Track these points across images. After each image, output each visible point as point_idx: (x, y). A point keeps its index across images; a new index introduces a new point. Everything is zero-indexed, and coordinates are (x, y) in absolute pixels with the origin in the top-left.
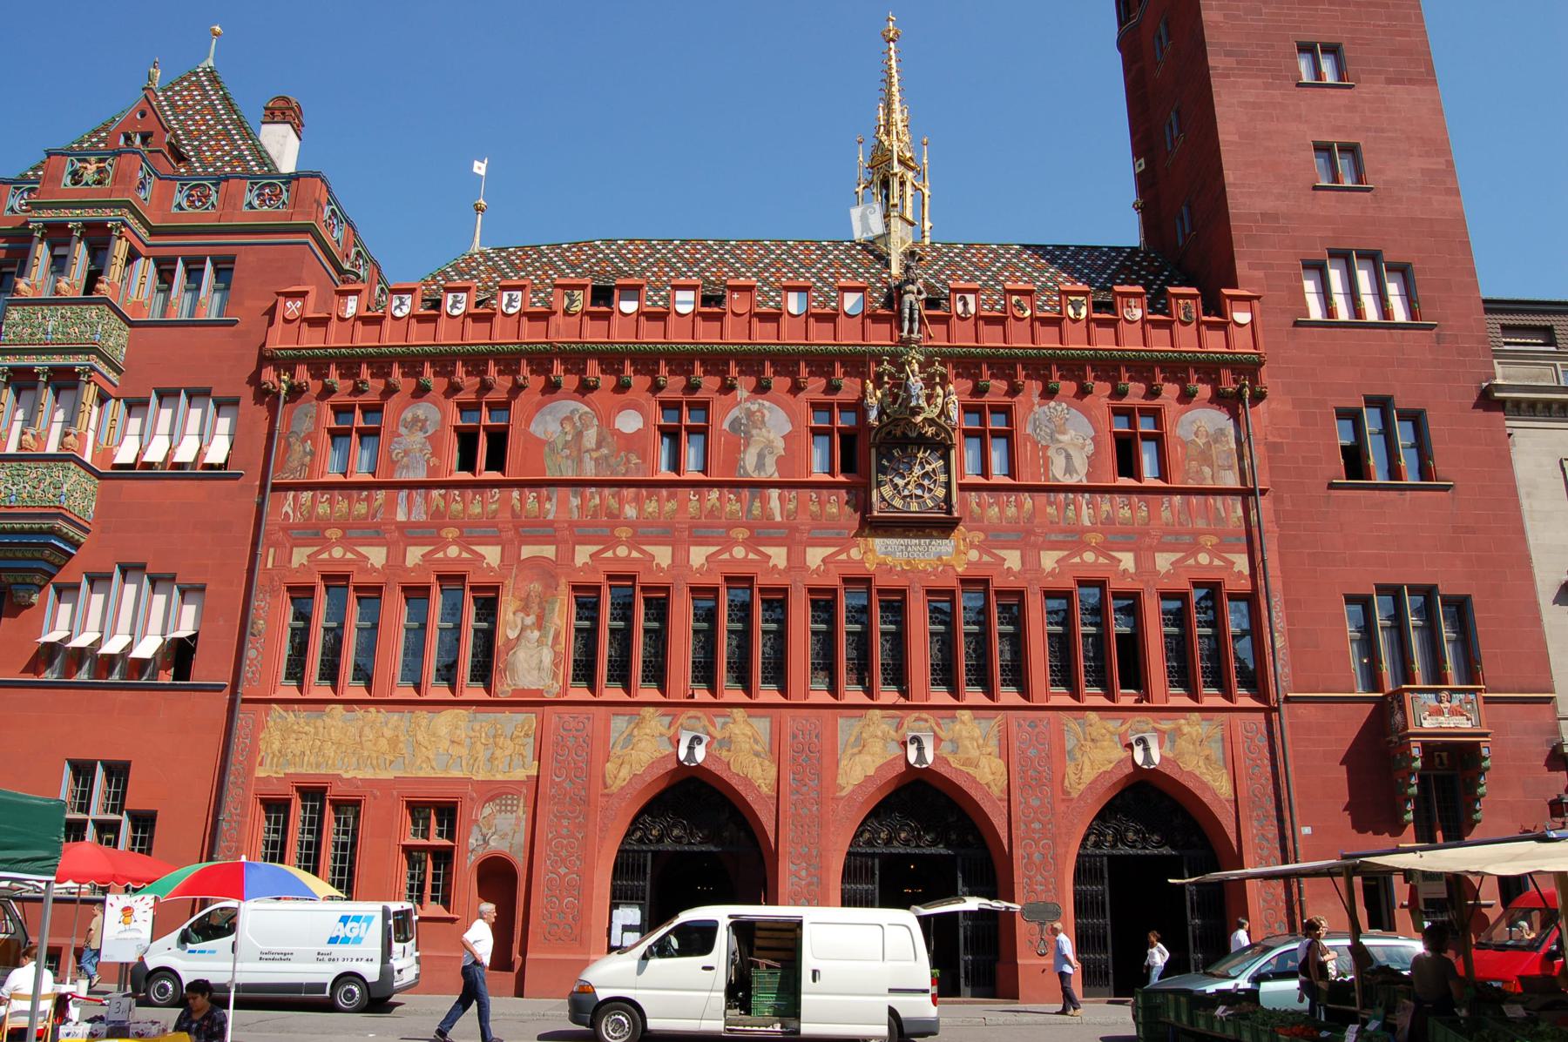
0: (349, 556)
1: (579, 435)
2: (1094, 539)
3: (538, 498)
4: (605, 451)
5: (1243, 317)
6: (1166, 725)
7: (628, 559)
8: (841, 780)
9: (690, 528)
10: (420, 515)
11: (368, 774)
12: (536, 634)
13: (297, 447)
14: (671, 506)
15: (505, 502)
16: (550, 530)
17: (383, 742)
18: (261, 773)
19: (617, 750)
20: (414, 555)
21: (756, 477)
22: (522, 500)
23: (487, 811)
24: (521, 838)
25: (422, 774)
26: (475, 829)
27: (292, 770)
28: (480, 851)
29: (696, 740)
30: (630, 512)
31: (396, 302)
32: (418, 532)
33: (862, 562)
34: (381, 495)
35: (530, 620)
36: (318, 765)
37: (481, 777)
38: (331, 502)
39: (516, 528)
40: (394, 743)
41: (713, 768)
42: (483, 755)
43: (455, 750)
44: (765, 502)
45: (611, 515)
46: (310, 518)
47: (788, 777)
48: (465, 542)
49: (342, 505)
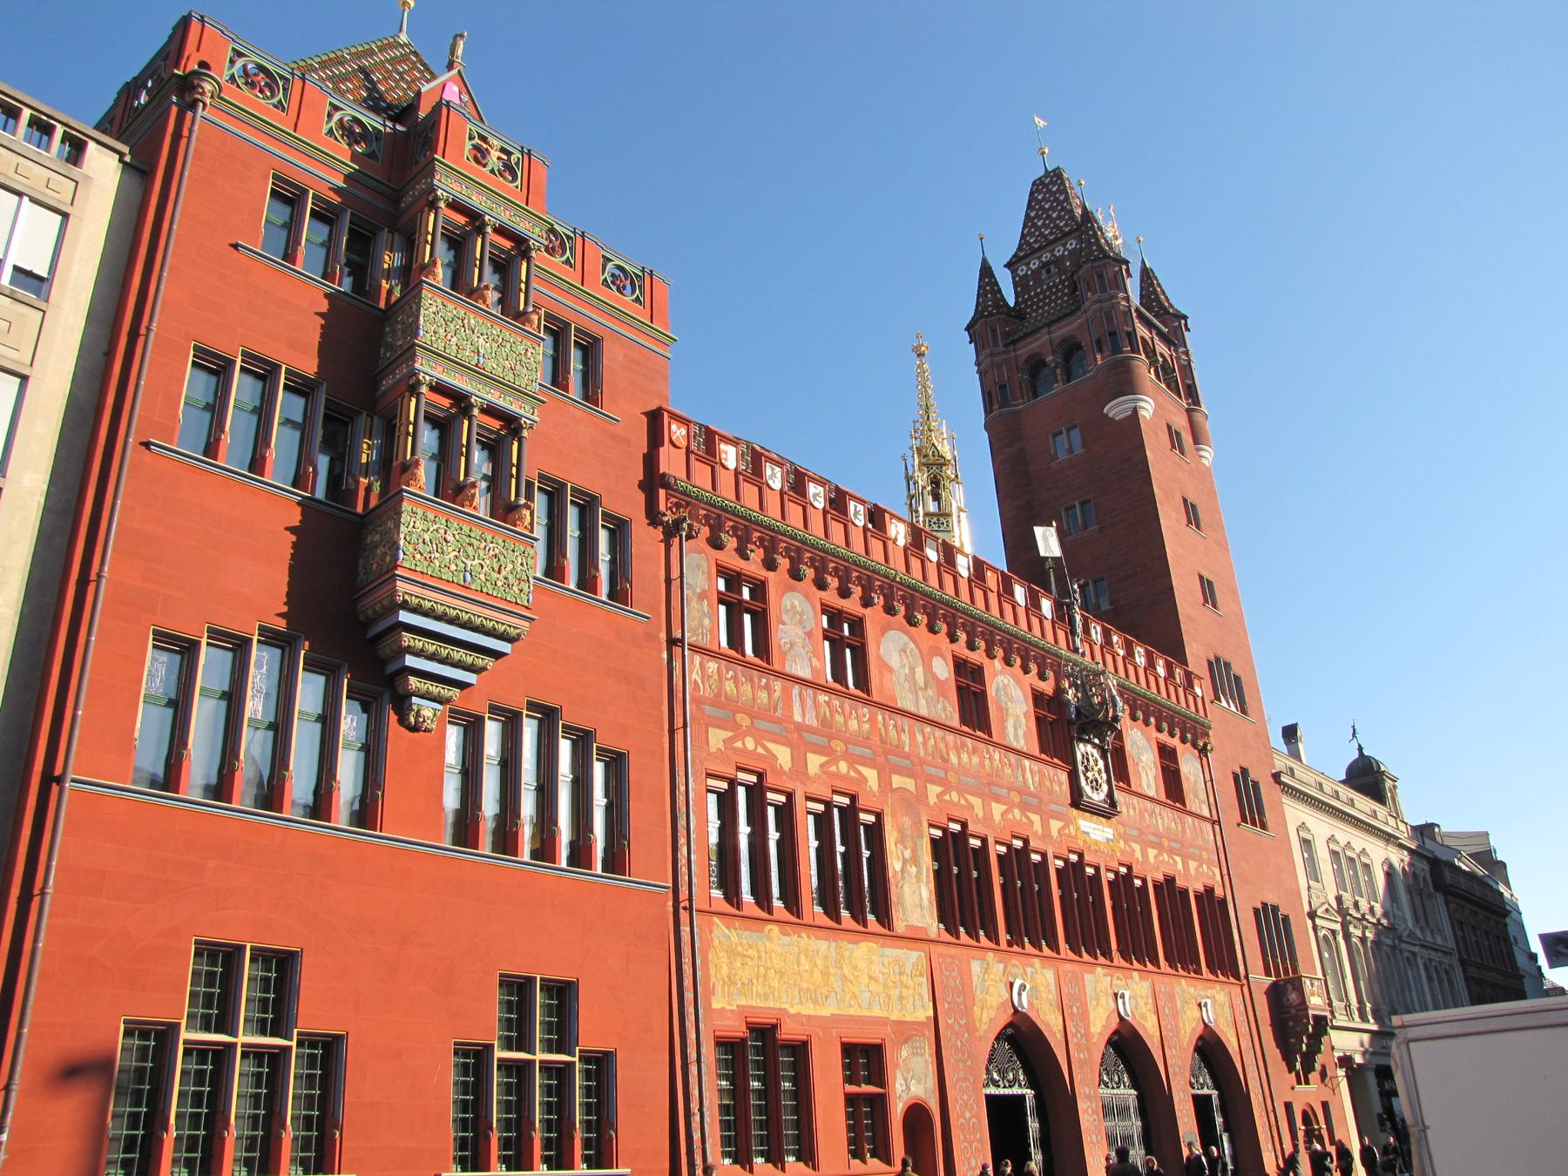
0: (760, 750)
1: (912, 670)
2: (1165, 842)
3: (895, 726)
4: (930, 692)
5: (1198, 691)
6: (1209, 993)
7: (958, 804)
8: (1092, 1029)
9: (990, 784)
10: (811, 720)
11: (809, 1009)
12: (914, 869)
13: (694, 604)
14: (975, 760)
15: (873, 721)
16: (906, 763)
17: (817, 974)
18: (716, 1005)
19: (979, 995)
20: (814, 762)
21: (1015, 745)
22: (885, 725)
23: (904, 1053)
24: (931, 1082)
25: (852, 1012)
26: (899, 1074)
27: (743, 1002)
28: (905, 1097)
29: (1023, 987)
30: (954, 758)
31: (769, 472)
32: (812, 738)
33: (1075, 837)
34: (778, 685)
35: (908, 854)
36: (766, 997)
37: (895, 1017)
38: (735, 678)
39: (886, 753)
40: (825, 973)
41: (1033, 1015)
42: (895, 993)
43: (874, 987)
44: (1023, 770)
45: (942, 757)
46: (718, 695)
47: (1071, 1028)
48: (853, 760)
49: (747, 688)
